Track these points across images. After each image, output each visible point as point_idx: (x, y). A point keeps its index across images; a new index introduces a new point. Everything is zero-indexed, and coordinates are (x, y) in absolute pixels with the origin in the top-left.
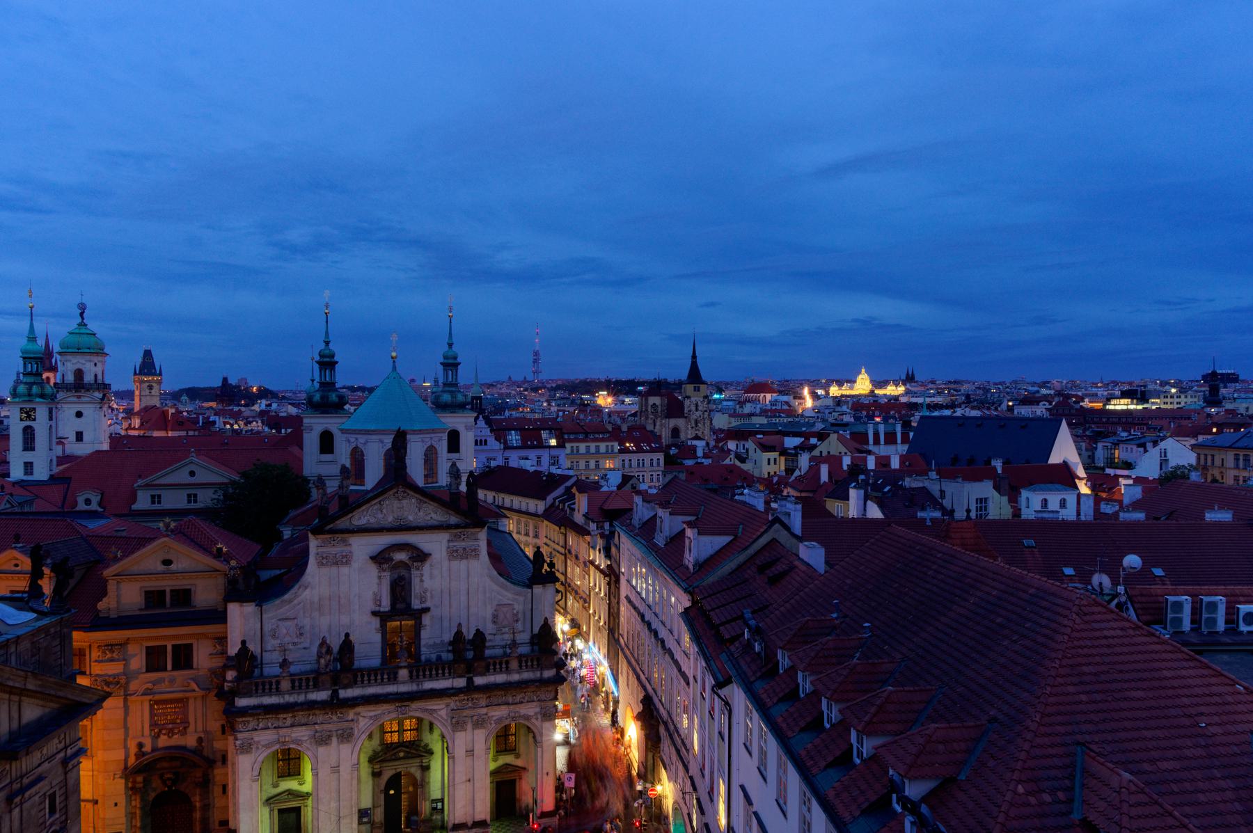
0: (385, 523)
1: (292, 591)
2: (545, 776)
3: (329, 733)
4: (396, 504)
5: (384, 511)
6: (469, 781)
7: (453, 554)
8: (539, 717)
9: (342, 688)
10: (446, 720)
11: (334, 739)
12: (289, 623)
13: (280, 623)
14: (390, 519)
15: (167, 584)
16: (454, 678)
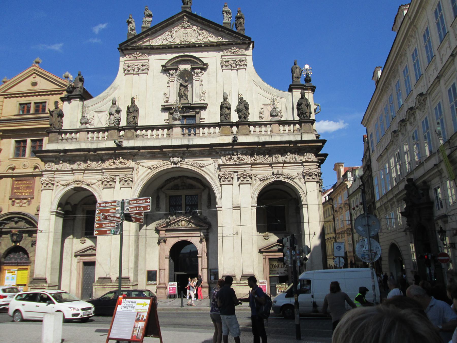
0: (175, 44)
1: (106, 91)
2: (312, 236)
3: (112, 177)
4: (182, 31)
5: (174, 35)
6: (237, 233)
7: (225, 65)
8: (302, 176)
9: (125, 140)
10: (214, 174)
11: (118, 185)
12: (100, 115)
13: (95, 114)
14: (178, 42)
15: (33, 100)
16: (221, 136)
